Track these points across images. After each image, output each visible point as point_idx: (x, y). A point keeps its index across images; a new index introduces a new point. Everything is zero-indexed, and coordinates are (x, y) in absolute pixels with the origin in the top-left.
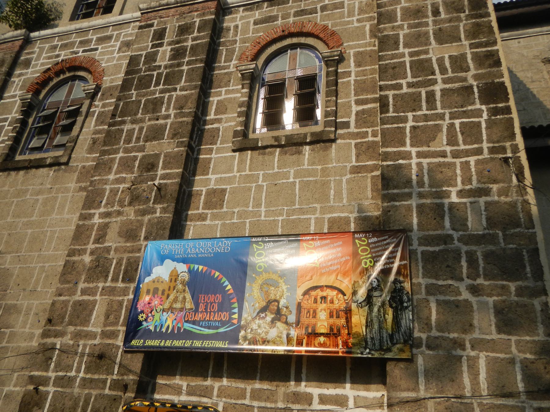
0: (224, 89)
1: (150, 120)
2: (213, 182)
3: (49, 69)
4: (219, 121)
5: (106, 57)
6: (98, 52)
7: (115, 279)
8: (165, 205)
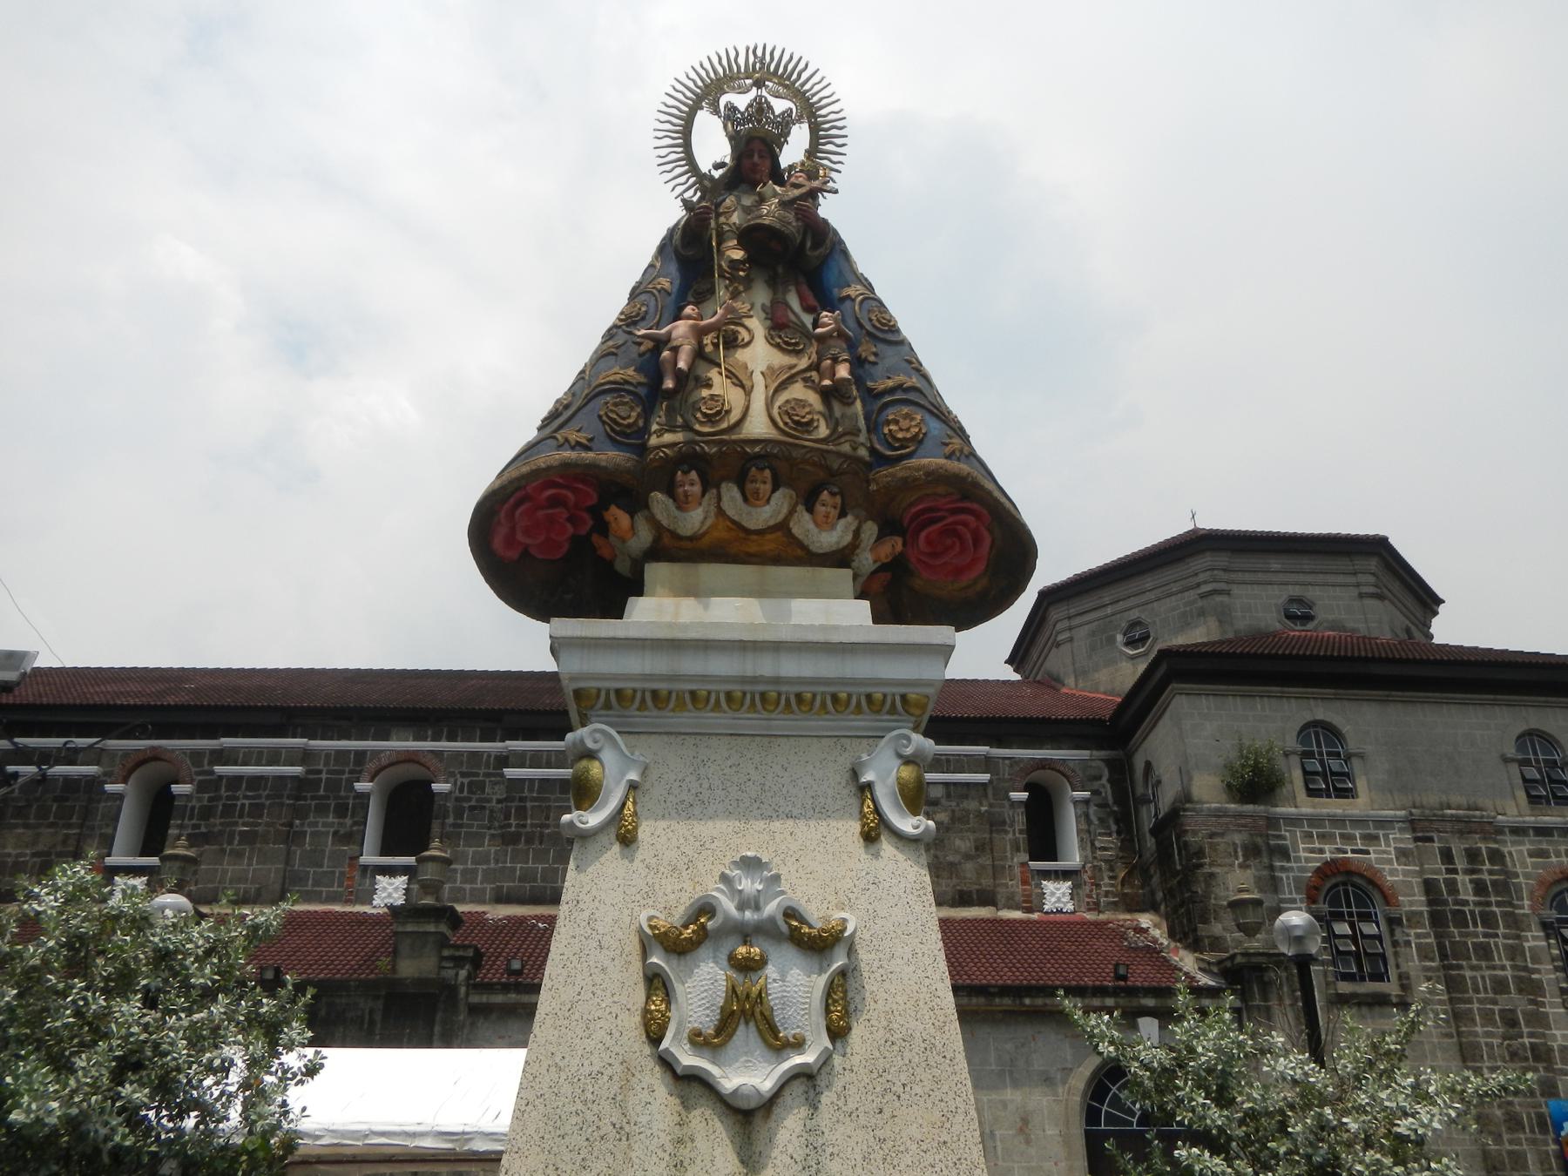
0: (1529, 934)
1: (1488, 968)
2: (1559, 1039)
3: (1319, 868)
4: (1538, 971)
5: (1387, 867)
6: (1373, 856)
7: (1532, 1131)
8: (1545, 1065)
